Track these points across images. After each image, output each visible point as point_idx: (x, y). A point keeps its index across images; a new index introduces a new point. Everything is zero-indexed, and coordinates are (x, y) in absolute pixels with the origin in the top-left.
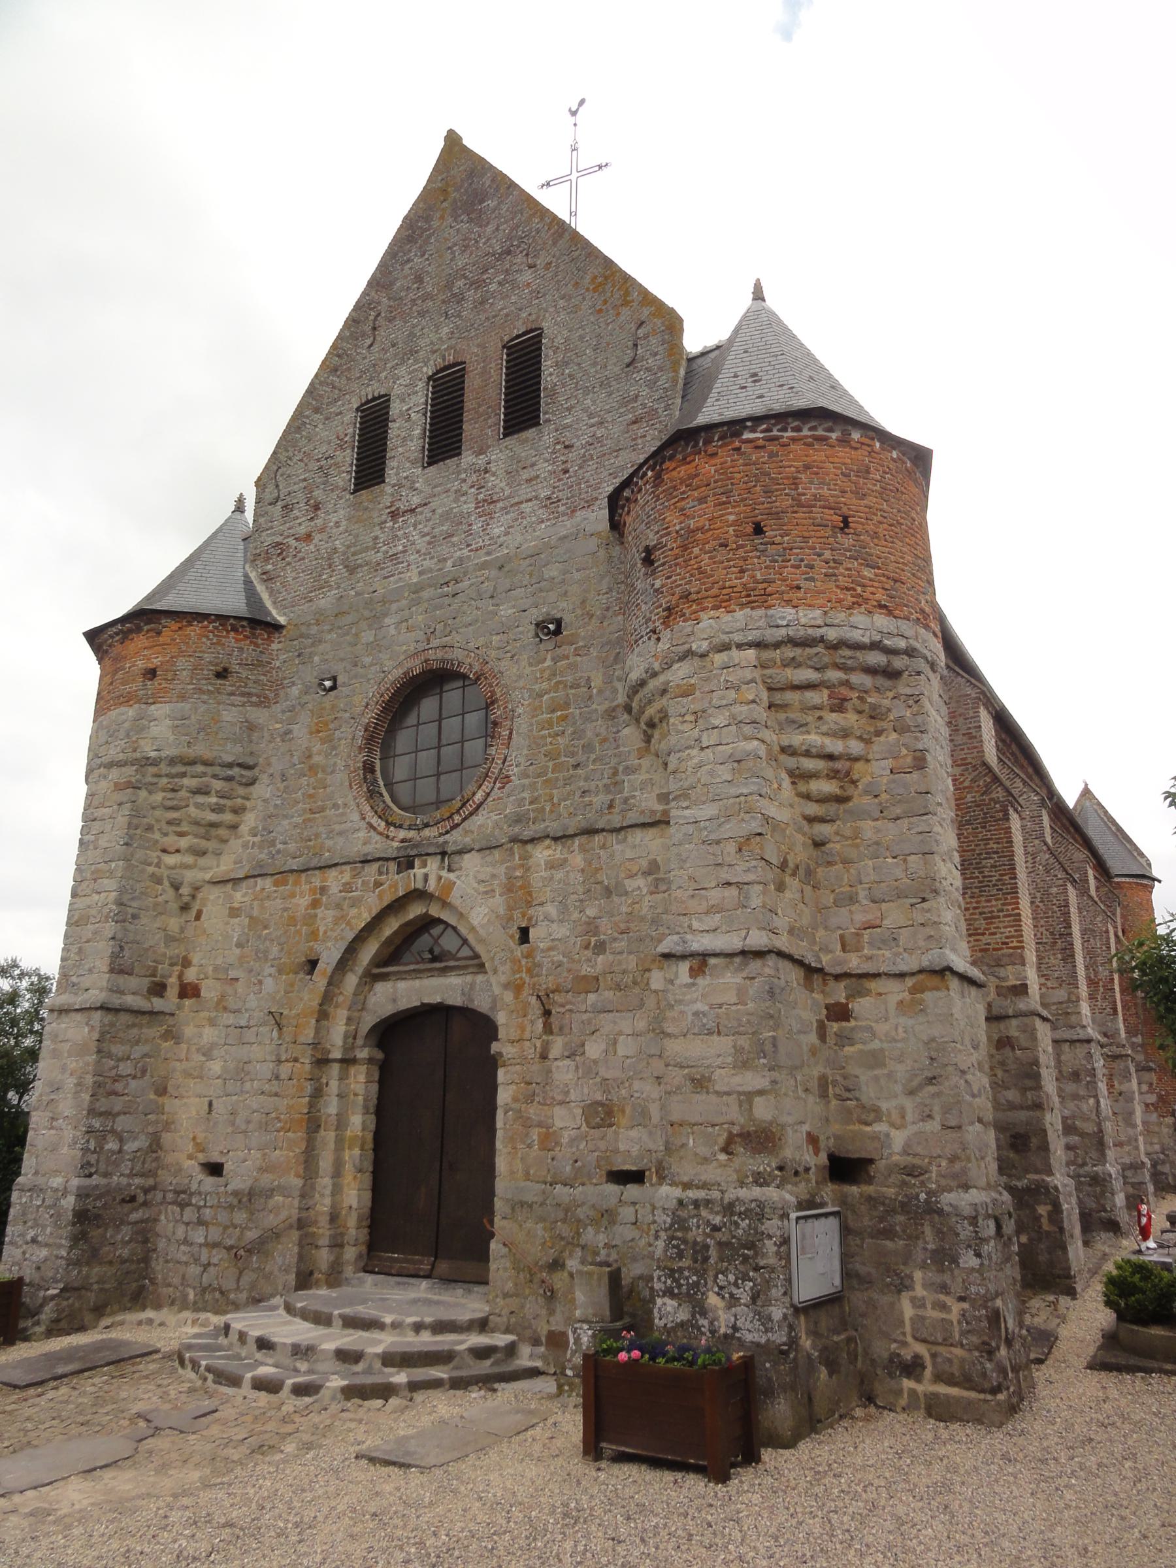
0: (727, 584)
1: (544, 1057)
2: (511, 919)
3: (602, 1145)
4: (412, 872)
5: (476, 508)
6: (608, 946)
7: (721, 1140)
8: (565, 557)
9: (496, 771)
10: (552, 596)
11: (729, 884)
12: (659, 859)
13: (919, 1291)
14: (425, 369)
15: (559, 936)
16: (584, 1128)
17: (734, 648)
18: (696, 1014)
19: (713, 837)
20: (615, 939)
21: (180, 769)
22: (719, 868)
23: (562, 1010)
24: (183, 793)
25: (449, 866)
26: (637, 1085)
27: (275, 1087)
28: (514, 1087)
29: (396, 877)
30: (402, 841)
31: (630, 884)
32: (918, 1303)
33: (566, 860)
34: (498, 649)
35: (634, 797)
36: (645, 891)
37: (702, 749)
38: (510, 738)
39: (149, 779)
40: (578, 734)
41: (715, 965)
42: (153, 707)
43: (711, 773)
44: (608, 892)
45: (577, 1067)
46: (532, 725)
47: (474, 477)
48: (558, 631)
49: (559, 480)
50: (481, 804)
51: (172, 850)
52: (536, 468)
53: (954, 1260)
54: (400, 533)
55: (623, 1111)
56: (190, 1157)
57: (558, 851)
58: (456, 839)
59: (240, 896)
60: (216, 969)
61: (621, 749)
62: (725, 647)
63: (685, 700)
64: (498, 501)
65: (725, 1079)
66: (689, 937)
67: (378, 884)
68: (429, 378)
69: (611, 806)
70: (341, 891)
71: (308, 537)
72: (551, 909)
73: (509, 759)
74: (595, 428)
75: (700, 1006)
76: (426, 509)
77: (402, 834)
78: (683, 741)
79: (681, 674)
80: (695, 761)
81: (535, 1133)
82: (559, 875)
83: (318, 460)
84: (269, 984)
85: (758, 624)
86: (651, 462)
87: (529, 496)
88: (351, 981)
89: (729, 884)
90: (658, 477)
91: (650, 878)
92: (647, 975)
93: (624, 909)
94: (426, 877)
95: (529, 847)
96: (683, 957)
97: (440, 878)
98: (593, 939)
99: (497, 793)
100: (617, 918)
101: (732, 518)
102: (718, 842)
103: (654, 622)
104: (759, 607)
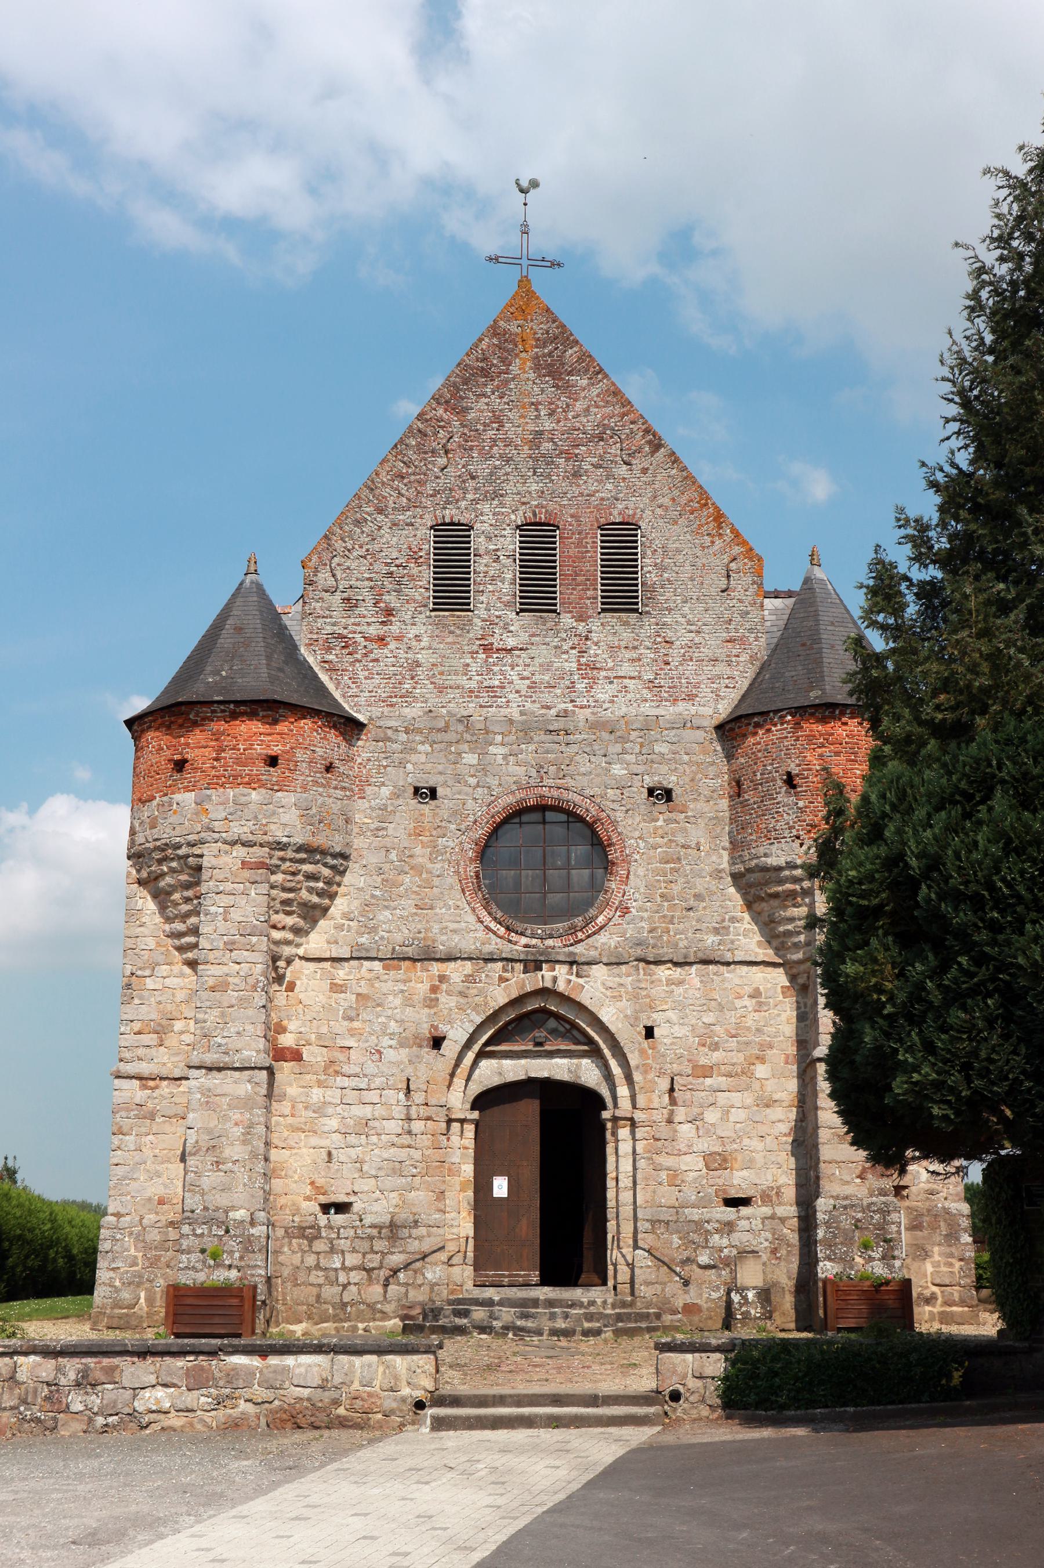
1: (670, 1121)
2: (637, 1019)
3: (720, 1182)
4: (540, 974)
5: (579, 669)
7: (858, 1172)
8: (674, 740)
9: (617, 902)
13: (937, 1258)
16: (705, 1170)
20: (727, 1041)
21: (304, 856)
24: (300, 877)
25: (577, 973)
26: (746, 1141)
27: (406, 1140)
28: (645, 1142)
29: (522, 976)
30: (526, 946)
31: (739, 1003)
32: (936, 1265)
34: (613, 801)
35: (739, 940)
36: (750, 1009)
39: (275, 861)
42: (279, 794)
45: (698, 1128)
47: (576, 640)
49: (661, 669)
50: (601, 928)
51: (279, 926)
53: (958, 1239)
54: (496, 669)
55: (736, 1159)
56: (308, 1199)
59: (342, 973)
60: (320, 1036)
67: (502, 979)
70: (463, 981)
71: (381, 640)
76: (523, 654)
77: (524, 940)
81: (664, 1175)
83: (387, 564)
84: (390, 1055)
87: (632, 674)
88: (470, 1056)
91: (754, 1001)
92: (752, 1067)
93: (733, 1020)
94: (555, 979)
95: (652, 967)
97: (570, 981)
99: (616, 920)
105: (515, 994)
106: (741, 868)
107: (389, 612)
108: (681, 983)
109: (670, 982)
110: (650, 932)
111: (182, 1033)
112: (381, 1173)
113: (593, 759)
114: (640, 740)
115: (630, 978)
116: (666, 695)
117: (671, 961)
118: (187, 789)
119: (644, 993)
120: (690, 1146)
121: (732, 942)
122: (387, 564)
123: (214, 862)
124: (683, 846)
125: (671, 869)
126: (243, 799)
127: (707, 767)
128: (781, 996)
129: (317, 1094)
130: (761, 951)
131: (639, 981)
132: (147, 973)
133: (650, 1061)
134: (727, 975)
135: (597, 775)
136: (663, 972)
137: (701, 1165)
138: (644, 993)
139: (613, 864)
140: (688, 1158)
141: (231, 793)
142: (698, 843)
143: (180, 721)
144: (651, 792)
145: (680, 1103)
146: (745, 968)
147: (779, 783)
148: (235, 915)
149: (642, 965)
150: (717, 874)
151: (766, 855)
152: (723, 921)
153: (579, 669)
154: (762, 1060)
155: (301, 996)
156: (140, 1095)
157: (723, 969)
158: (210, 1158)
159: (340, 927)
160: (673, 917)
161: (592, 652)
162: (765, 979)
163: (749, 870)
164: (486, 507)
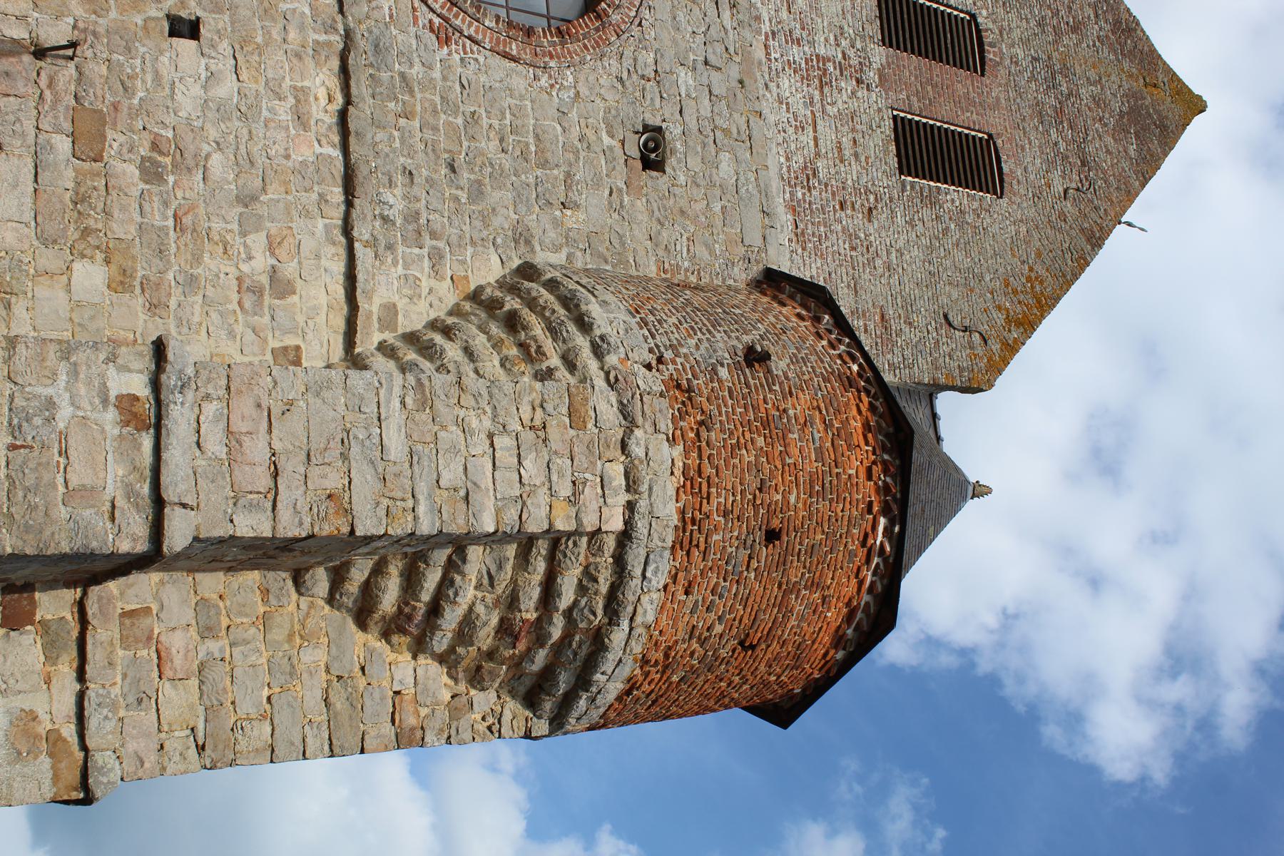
0: (713, 490)
5: (817, 56)
6: (155, 189)
8: (743, 191)
9: (458, 22)
10: (694, 163)
11: (276, 475)
12: (295, 298)
14: (984, 13)
15: (179, 97)
17: (628, 497)
18: (50, 404)
19: (355, 450)
20: (166, 204)
22: (303, 457)
23: (43, 81)
31: (257, 241)
33: (306, 127)
34: (635, 60)
35: (395, 263)
36: (245, 268)
37: (491, 436)
38: (506, 56)
40: (498, 176)
41: (138, 447)
43: (454, 450)
44: (246, 200)
46: (522, 98)
47: (854, 62)
48: (647, 164)
49: (833, 194)
52: (853, 159)
57: (321, 115)
61: (470, 250)
62: (631, 484)
63: (564, 410)
64: (822, 92)
66: (190, 395)
68: (973, 16)
69: (385, 219)
72: (226, 88)
73: (475, 48)
74: (885, 258)
75: (64, 413)
78: (504, 403)
79: (603, 407)
80: (475, 423)
82: (284, 111)
85: (655, 536)
86: (869, 374)
87: (821, 142)
89: (276, 475)
90: (849, 383)
91: (265, 280)
92: (99, 256)
93: (217, 225)
95: (335, 63)
96: (156, 385)
98: (168, 160)
100: (201, 211)
101: (793, 499)
102: (344, 457)
103: (674, 362)
104: (677, 537)
108: (301, 119)
109: (301, 95)
110: (403, 76)
113: (700, 39)
114: (734, 131)
115: (307, 11)
116: (800, 195)
117: (348, 101)
119: (276, 35)
121: (390, 247)
124: (568, 175)
125: (527, 144)
127: (707, 246)
128: (277, 345)
130: (375, 309)
131: (302, 27)
133: (113, 14)
134: (320, 223)
135: (674, 41)
136: (321, 83)
138: (276, 35)
142: (577, 206)
146: (339, 267)
149: (337, 41)
150: (522, 237)
152: (434, 235)
153: (817, 56)
154: (121, 283)
157: (337, 213)
160: (435, 129)
161: (843, 84)
162: (315, 308)
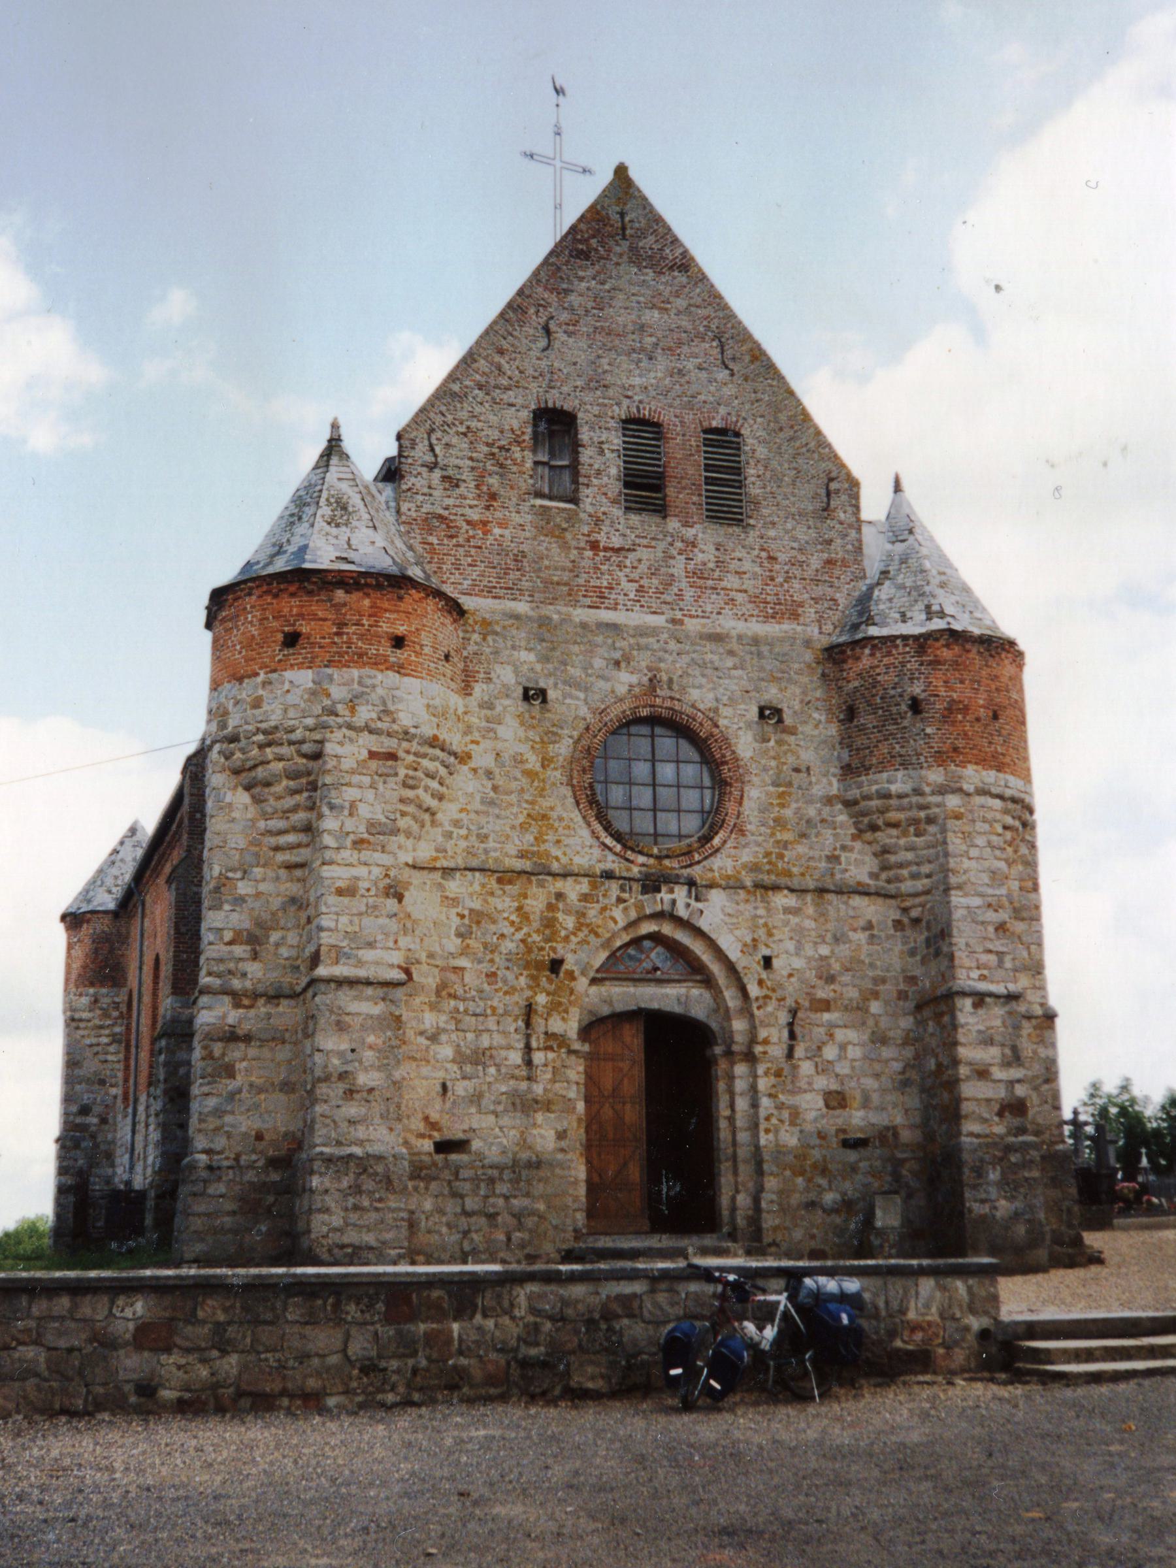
3: (840, 1121)
4: (659, 896)
16: (825, 1110)
24: (420, 774)
50: (718, 850)
54: (604, 568)
56: (422, 1136)
58: (696, 872)
60: (431, 956)
65: (998, 1073)
72: (790, 946)
77: (641, 859)
81: (786, 1114)
82: (794, 920)
94: (674, 902)
105: (633, 915)
106: (854, 793)
107: (493, 496)
109: (787, 910)
111: (277, 945)
112: (500, 1108)
118: (300, 666)
120: (810, 1084)
122: (488, 444)
123: (339, 750)
126: (369, 682)
129: (430, 1020)
132: (239, 875)
136: (782, 900)
137: (821, 1103)
139: (727, 784)
140: (808, 1096)
141: (355, 673)
143: (292, 589)
144: (761, 710)
145: (799, 1037)
147: (904, 708)
148: (364, 810)
150: (829, 801)
151: (889, 782)
154: (876, 995)
155: (409, 909)
156: (233, 1016)
158: (341, 1087)
159: (449, 835)
163: (867, 798)
164: (588, 397)
